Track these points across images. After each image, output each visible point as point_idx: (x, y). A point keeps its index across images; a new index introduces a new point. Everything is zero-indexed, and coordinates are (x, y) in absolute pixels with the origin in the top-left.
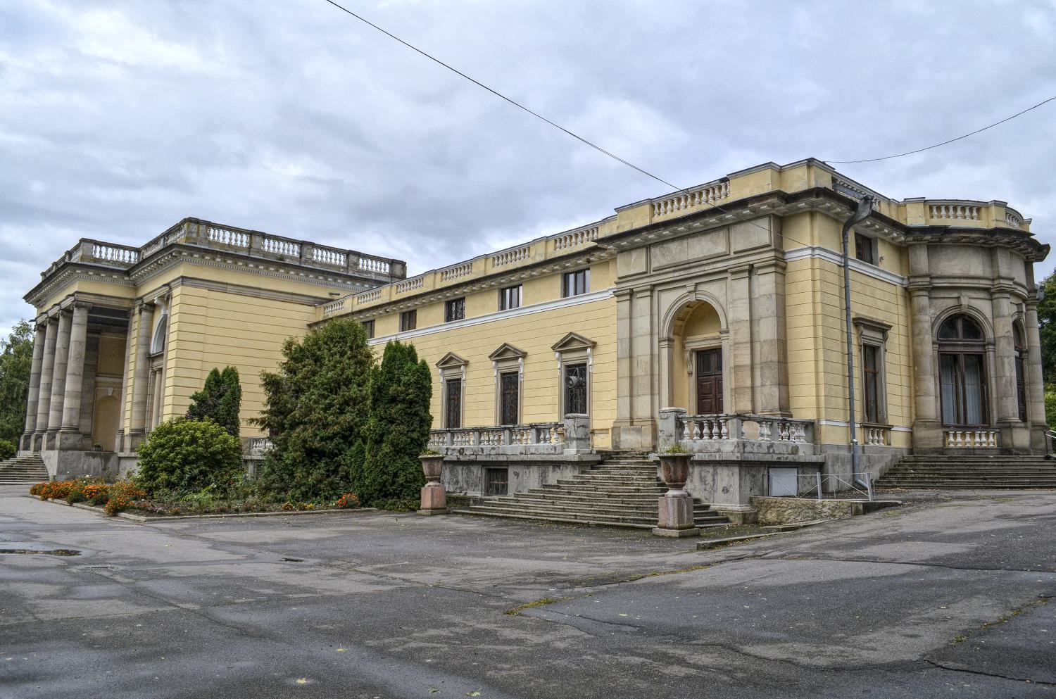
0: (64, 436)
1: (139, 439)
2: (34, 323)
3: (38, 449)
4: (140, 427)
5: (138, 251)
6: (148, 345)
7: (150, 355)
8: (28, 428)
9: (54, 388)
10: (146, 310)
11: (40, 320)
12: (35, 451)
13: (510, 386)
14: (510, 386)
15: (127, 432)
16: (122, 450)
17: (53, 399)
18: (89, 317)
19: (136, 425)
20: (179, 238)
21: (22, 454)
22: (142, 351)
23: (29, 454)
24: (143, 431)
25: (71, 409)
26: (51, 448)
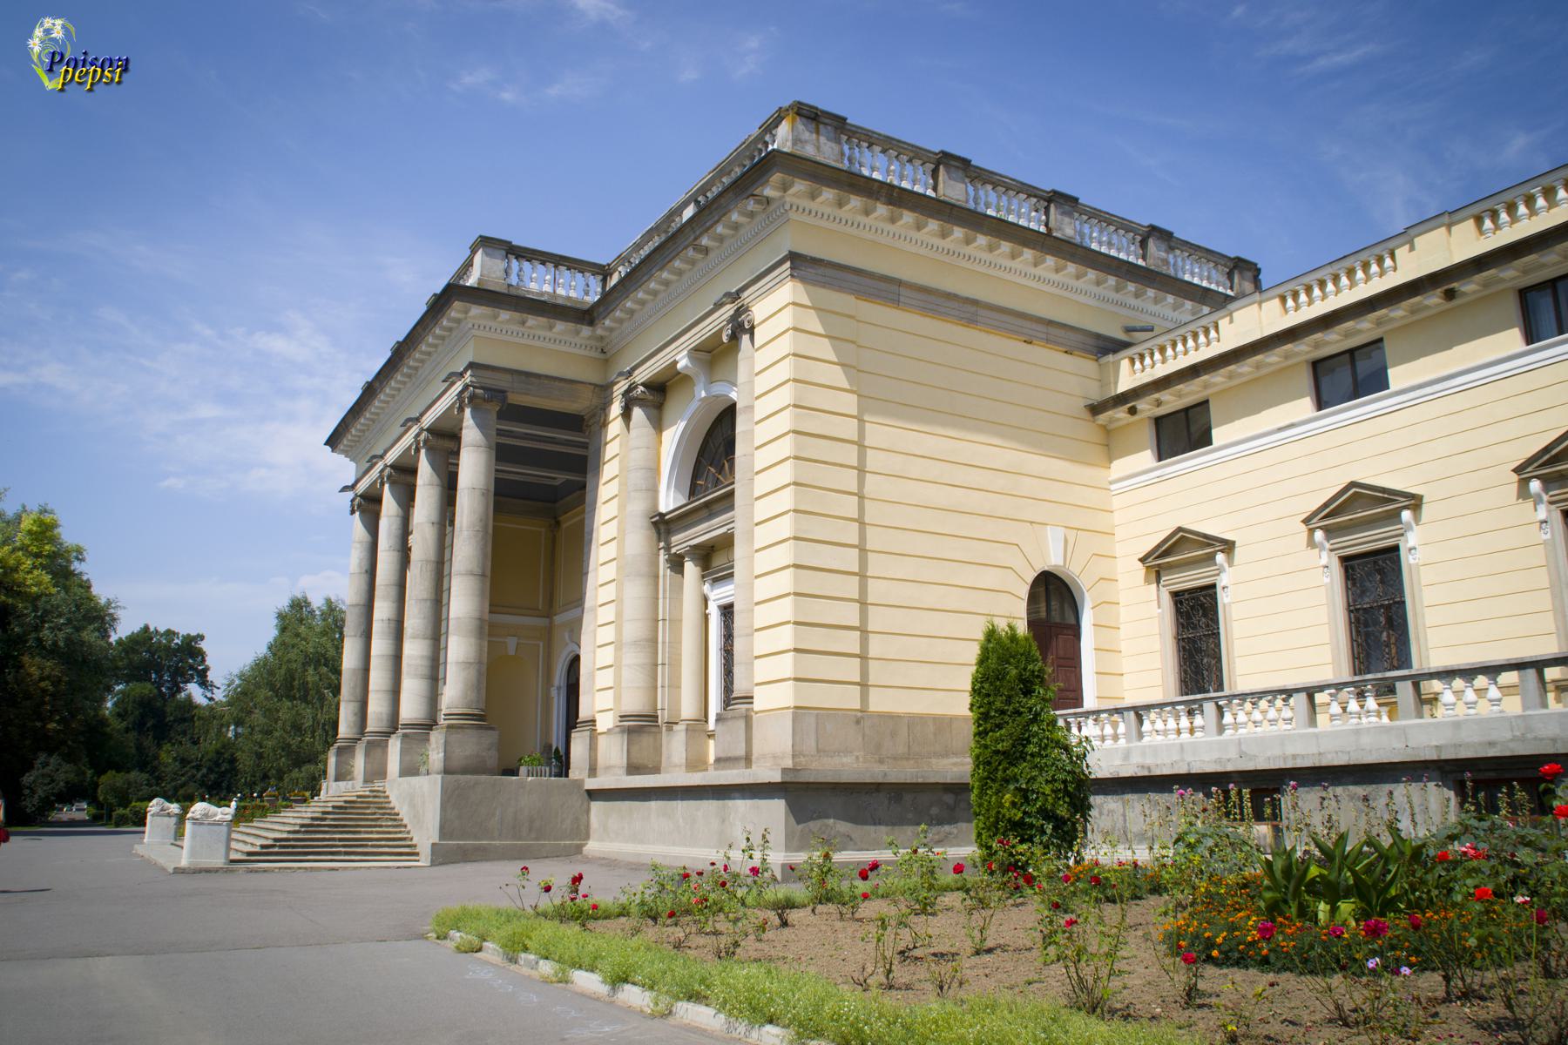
0: (456, 737)
1: (646, 740)
2: (350, 495)
3: (377, 772)
4: (646, 710)
5: (604, 272)
6: (653, 491)
7: (662, 515)
8: (344, 730)
9: (415, 620)
10: (640, 402)
11: (362, 487)
12: (366, 781)
13: (1196, 617)
14: (1196, 617)
15: (605, 723)
16: (593, 771)
17: (415, 650)
18: (498, 445)
19: (634, 703)
20: (783, 138)
21: (333, 791)
22: (638, 507)
23: (354, 787)
24: (654, 717)
25: (467, 664)
26: (409, 770)
